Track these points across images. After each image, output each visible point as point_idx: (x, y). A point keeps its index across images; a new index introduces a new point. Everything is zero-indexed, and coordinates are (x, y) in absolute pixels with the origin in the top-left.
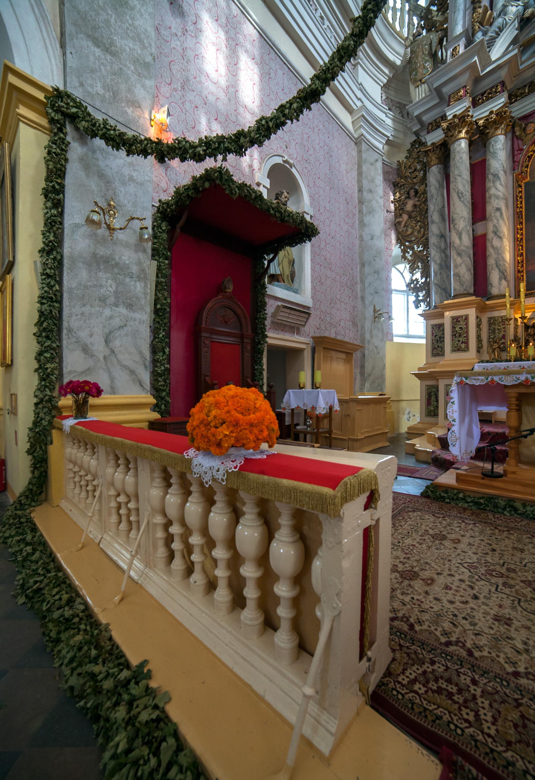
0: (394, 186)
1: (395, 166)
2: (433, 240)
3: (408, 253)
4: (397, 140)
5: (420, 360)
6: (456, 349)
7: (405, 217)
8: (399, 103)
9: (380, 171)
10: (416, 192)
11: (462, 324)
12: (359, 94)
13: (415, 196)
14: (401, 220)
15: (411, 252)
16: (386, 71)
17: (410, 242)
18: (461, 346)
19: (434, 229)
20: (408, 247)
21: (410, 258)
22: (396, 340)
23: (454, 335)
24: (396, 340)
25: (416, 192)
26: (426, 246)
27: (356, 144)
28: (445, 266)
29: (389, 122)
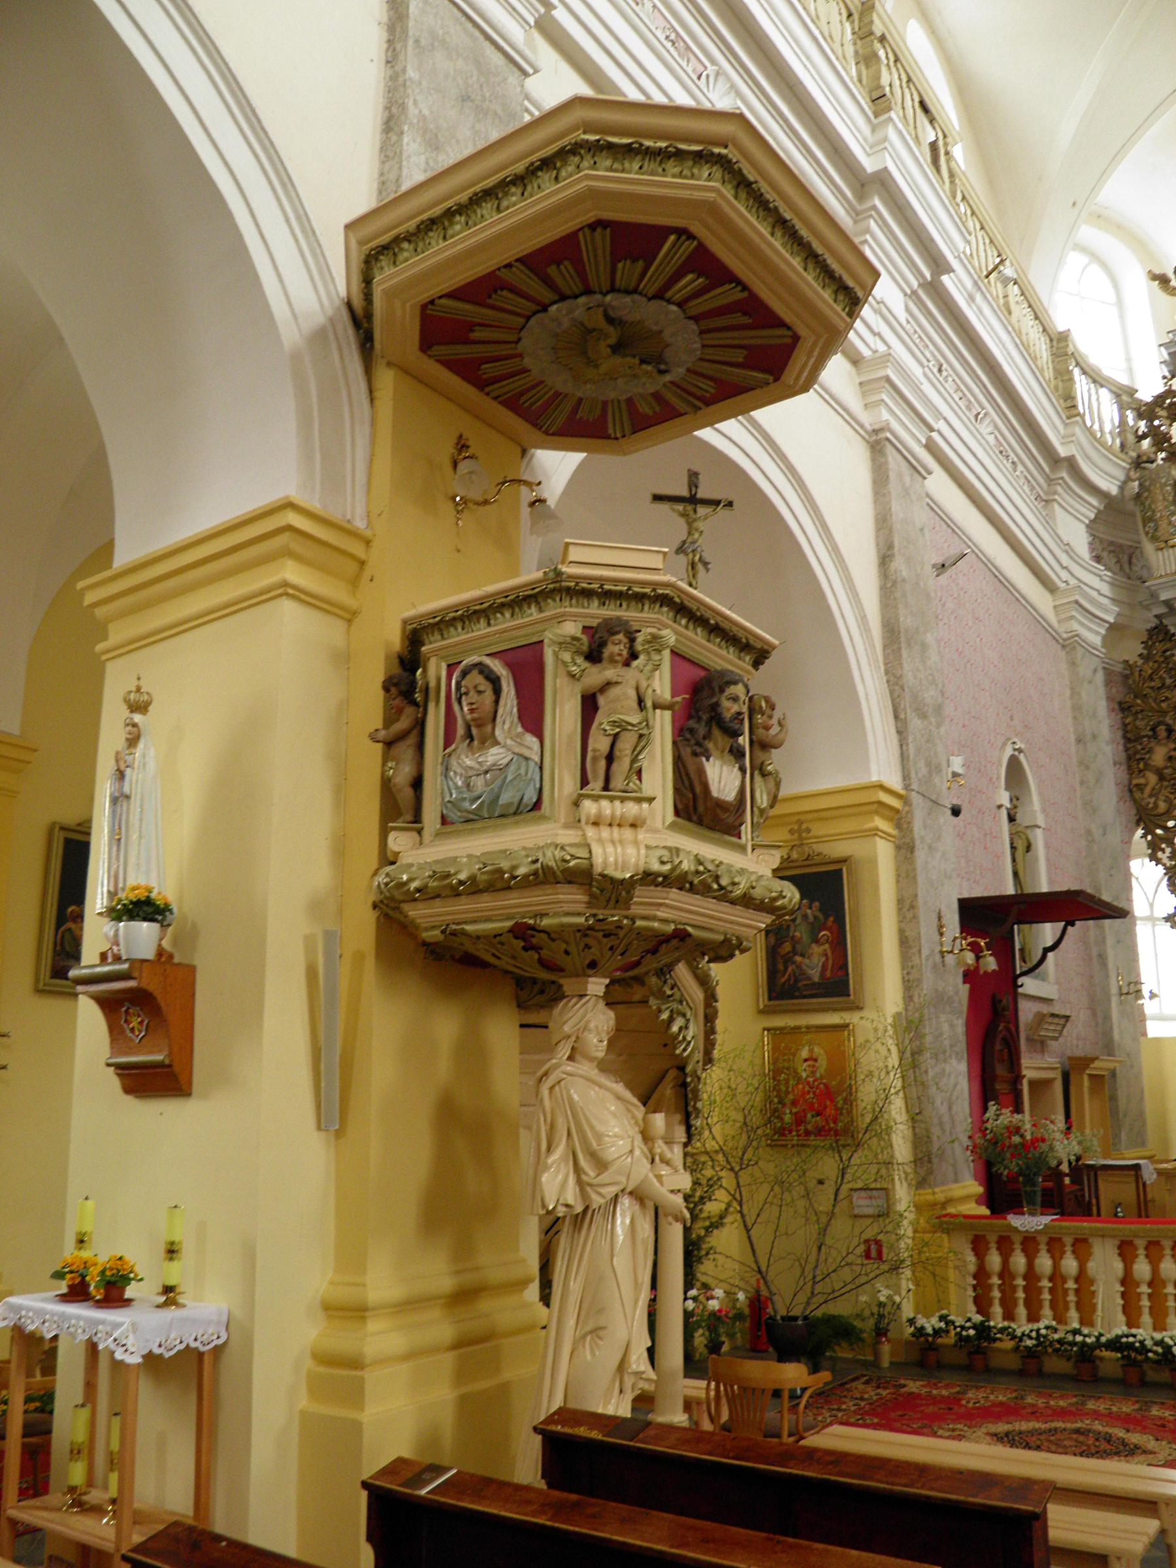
0: (1123, 710)
1: (1119, 668)
3: (1163, 851)
4: (1120, 621)
7: (1153, 779)
8: (1111, 543)
12: (1065, 560)
13: (1168, 737)
14: (1142, 781)
15: (1168, 850)
16: (1095, 502)
17: (1165, 828)
20: (1162, 839)
21: (1166, 861)
27: (1063, 646)
29: (1105, 589)
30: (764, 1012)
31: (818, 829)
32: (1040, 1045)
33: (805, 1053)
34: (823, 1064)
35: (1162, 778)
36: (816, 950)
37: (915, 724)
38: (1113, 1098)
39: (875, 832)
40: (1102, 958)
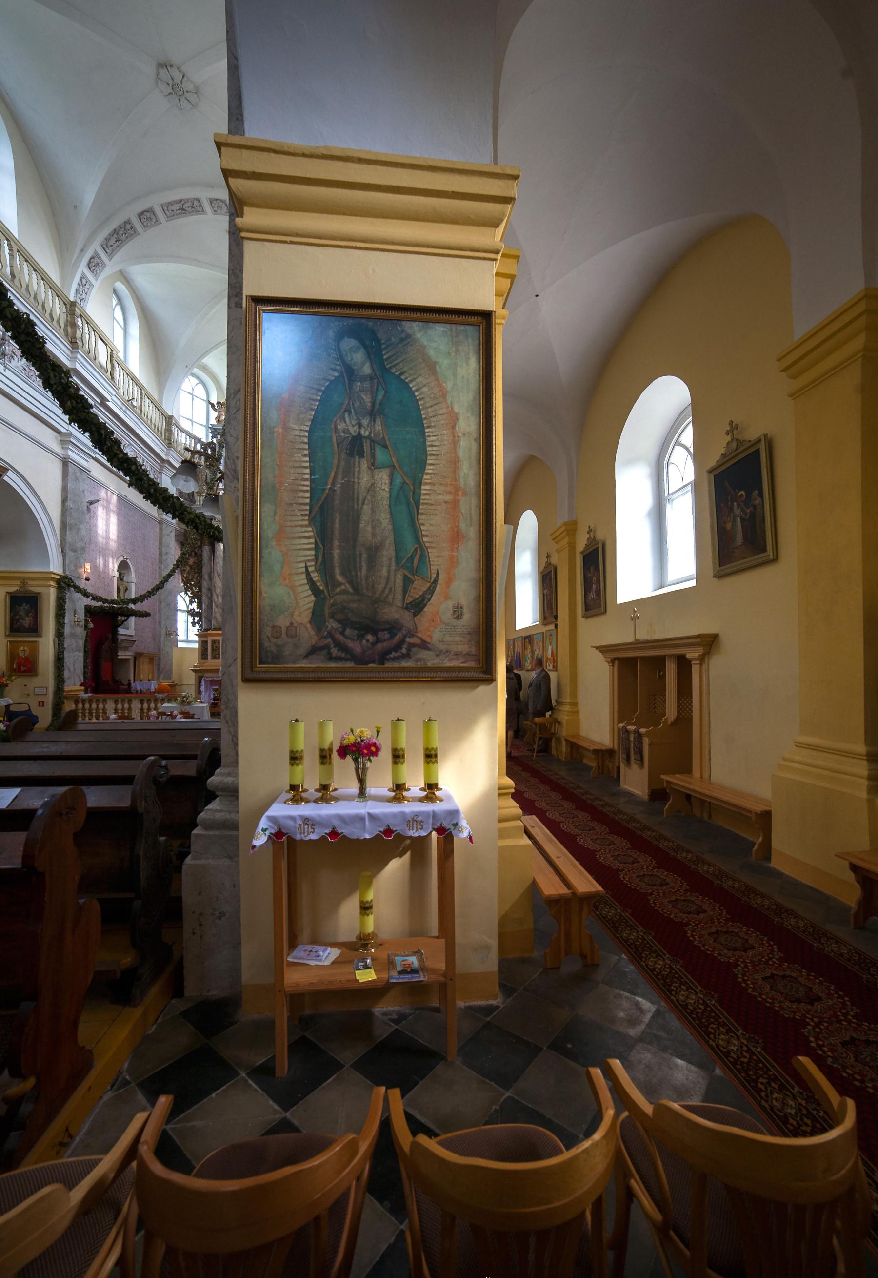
2: (204, 590)
5: (194, 660)
6: (214, 657)
7: (188, 568)
9: (173, 538)
10: (196, 554)
11: (217, 644)
18: (215, 656)
19: (205, 584)
22: (180, 645)
23: (213, 650)
24: (180, 645)
25: (196, 554)
26: (200, 589)
28: (210, 607)
30: (7, 636)
31: (30, 583)
32: (126, 649)
33: (22, 648)
34: (27, 653)
35: (191, 567)
36: (27, 619)
37: (70, 554)
38: (159, 665)
39: (50, 586)
40: (160, 623)
